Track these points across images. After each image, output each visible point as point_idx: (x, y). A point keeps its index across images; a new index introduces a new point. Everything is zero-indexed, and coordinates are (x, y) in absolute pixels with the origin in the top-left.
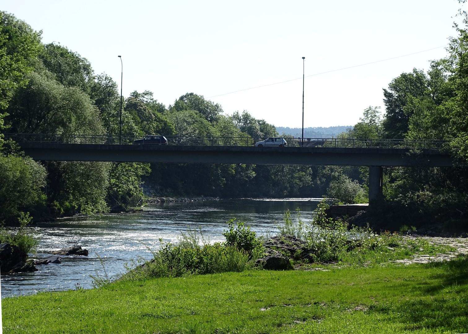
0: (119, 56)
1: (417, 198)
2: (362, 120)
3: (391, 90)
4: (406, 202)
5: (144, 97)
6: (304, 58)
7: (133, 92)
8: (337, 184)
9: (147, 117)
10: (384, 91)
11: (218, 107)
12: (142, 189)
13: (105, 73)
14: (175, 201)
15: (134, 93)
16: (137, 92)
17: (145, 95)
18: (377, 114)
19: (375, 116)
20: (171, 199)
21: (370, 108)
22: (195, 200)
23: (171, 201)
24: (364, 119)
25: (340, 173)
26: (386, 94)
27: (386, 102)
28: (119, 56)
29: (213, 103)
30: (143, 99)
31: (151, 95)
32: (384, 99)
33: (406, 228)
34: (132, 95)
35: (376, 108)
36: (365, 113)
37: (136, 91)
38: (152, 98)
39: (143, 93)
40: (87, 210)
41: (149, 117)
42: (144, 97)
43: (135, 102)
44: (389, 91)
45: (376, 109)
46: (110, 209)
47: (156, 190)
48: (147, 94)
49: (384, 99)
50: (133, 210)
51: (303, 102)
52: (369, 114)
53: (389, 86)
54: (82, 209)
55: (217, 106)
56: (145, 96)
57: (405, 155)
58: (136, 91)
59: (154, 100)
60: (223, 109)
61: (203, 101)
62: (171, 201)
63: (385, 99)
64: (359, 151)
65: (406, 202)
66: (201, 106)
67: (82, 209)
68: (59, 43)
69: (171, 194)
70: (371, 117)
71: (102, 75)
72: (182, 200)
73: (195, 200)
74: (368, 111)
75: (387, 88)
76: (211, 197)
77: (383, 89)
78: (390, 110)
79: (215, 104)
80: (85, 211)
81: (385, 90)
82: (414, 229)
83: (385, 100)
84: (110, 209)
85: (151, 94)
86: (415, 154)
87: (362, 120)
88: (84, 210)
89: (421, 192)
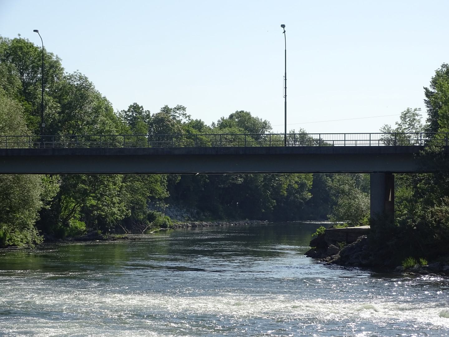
0: (35, 31)
1: (432, 217)
2: (399, 125)
3: (434, 88)
4: (414, 221)
5: (176, 113)
6: (283, 26)
7: (164, 106)
8: (348, 200)
9: (175, 133)
10: (425, 90)
11: (266, 124)
12: (129, 212)
13: (79, 72)
14: (210, 226)
15: (165, 108)
16: (168, 106)
17: (177, 110)
18: (416, 117)
19: (415, 119)
20: (204, 223)
21: (408, 110)
22: (236, 224)
23: (204, 226)
24: (402, 124)
25: (352, 186)
26: (428, 94)
27: (427, 102)
28: (35, 31)
29: (261, 120)
30: (175, 114)
31: (184, 110)
32: (425, 100)
33: (411, 262)
34: (163, 110)
35: (415, 110)
36: (402, 116)
37: (167, 106)
38: (185, 112)
39: (175, 108)
40: (14, 240)
41: (178, 133)
42: (176, 113)
43: (162, 117)
44: (431, 90)
45: (416, 112)
46: (43, 238)
47: (192, 214)
48: (180, 108)
49: (425, 100)
50: (113, 237)
51: (286, 88)
52: (407, 117)
53: (431, 84)
54: (7, 239)
55: (265, 123)
56: (178, 111)
57: (418, 154)
58: (167, 106)
59: (187, 115)
60: (272, 125)
61: (250, 118)
62: (204, 226)
63: (426, 99)
64: (383, 161)
65: (414, 221)
66: (247, 123)
67: (7, 239)
68: (19, 35)
69: (210, 217)
70: (409, 121)
71: (76, 74)
72: (219, 224)
73: (236, 224)
74: (406, 114)
75: (428, 85)
76: (258, 220)
77: (424, 88)
78: (434, 115)
79: (263, 121)
80: (12, 241)
81: (426, 89)
82: (424, 263)
83: (426, 101)
84: (43, 238)
85: (184, 109)
86: (433, 153)
87: (399, 125)
88: (11, 239)
89: (436, 208)
